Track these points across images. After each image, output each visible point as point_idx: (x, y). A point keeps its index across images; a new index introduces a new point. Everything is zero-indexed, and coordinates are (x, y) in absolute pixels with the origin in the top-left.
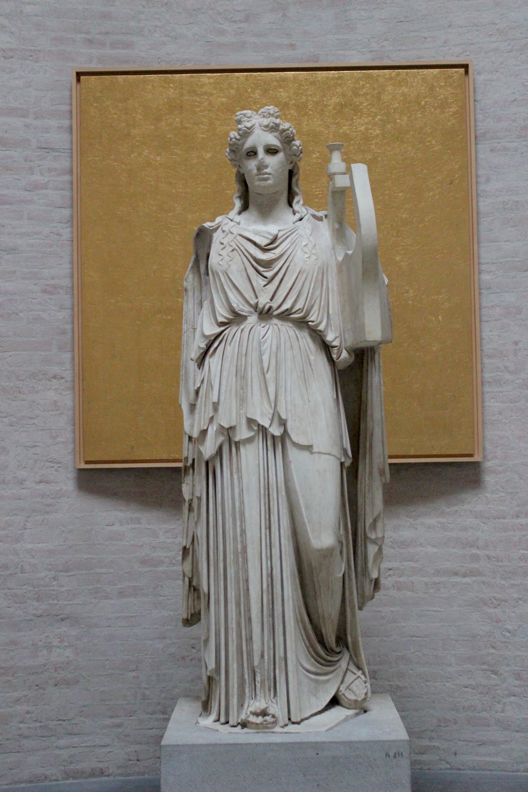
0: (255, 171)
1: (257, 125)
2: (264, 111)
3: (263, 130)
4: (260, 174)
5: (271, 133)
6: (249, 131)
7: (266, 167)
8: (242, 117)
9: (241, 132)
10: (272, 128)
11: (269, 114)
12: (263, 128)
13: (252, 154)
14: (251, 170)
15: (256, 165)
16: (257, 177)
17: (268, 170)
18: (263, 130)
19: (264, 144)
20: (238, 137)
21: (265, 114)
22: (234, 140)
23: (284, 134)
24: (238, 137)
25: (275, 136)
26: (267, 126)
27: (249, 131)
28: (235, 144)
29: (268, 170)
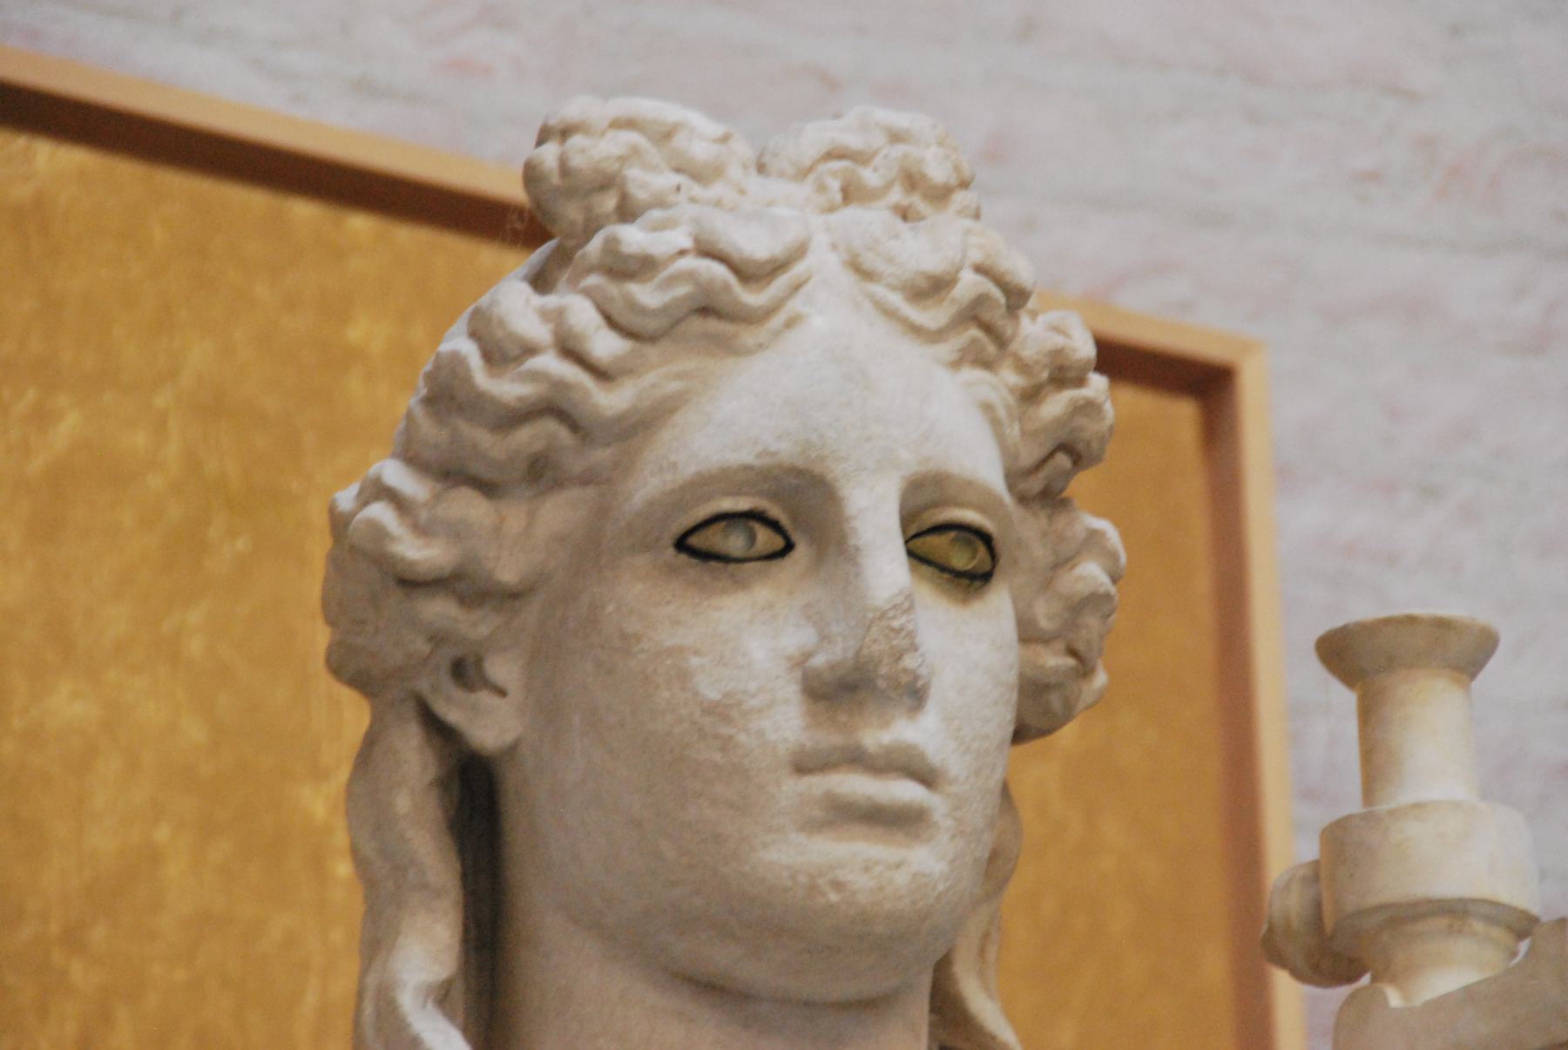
0: (786, 723)
1: (823, 262)
2: (853, 141)
3: (889, 313)
4: (857, 759)
5: (956, 365)
6: (752, 298)
7: (915, 694)
8: (634, 153)
9: (648, 295)
10: (973, 314)
11: (912, 180)
12: (896, 300)
13: (765, 539)
14: (721, 711)
15: (800, 662)
16: (792, 788)
17: (919, 732)
18: (889, 313)
19: (910, 461)
20: (605, 345)
21: (871, 177)
22: (551, 363)
23: (1055, 405)
24: (605, 345)
25: (987, 408)
26: (934, 287)
27: (752, 298)
28: (554, 407)
29: (919, 732)
